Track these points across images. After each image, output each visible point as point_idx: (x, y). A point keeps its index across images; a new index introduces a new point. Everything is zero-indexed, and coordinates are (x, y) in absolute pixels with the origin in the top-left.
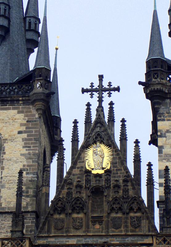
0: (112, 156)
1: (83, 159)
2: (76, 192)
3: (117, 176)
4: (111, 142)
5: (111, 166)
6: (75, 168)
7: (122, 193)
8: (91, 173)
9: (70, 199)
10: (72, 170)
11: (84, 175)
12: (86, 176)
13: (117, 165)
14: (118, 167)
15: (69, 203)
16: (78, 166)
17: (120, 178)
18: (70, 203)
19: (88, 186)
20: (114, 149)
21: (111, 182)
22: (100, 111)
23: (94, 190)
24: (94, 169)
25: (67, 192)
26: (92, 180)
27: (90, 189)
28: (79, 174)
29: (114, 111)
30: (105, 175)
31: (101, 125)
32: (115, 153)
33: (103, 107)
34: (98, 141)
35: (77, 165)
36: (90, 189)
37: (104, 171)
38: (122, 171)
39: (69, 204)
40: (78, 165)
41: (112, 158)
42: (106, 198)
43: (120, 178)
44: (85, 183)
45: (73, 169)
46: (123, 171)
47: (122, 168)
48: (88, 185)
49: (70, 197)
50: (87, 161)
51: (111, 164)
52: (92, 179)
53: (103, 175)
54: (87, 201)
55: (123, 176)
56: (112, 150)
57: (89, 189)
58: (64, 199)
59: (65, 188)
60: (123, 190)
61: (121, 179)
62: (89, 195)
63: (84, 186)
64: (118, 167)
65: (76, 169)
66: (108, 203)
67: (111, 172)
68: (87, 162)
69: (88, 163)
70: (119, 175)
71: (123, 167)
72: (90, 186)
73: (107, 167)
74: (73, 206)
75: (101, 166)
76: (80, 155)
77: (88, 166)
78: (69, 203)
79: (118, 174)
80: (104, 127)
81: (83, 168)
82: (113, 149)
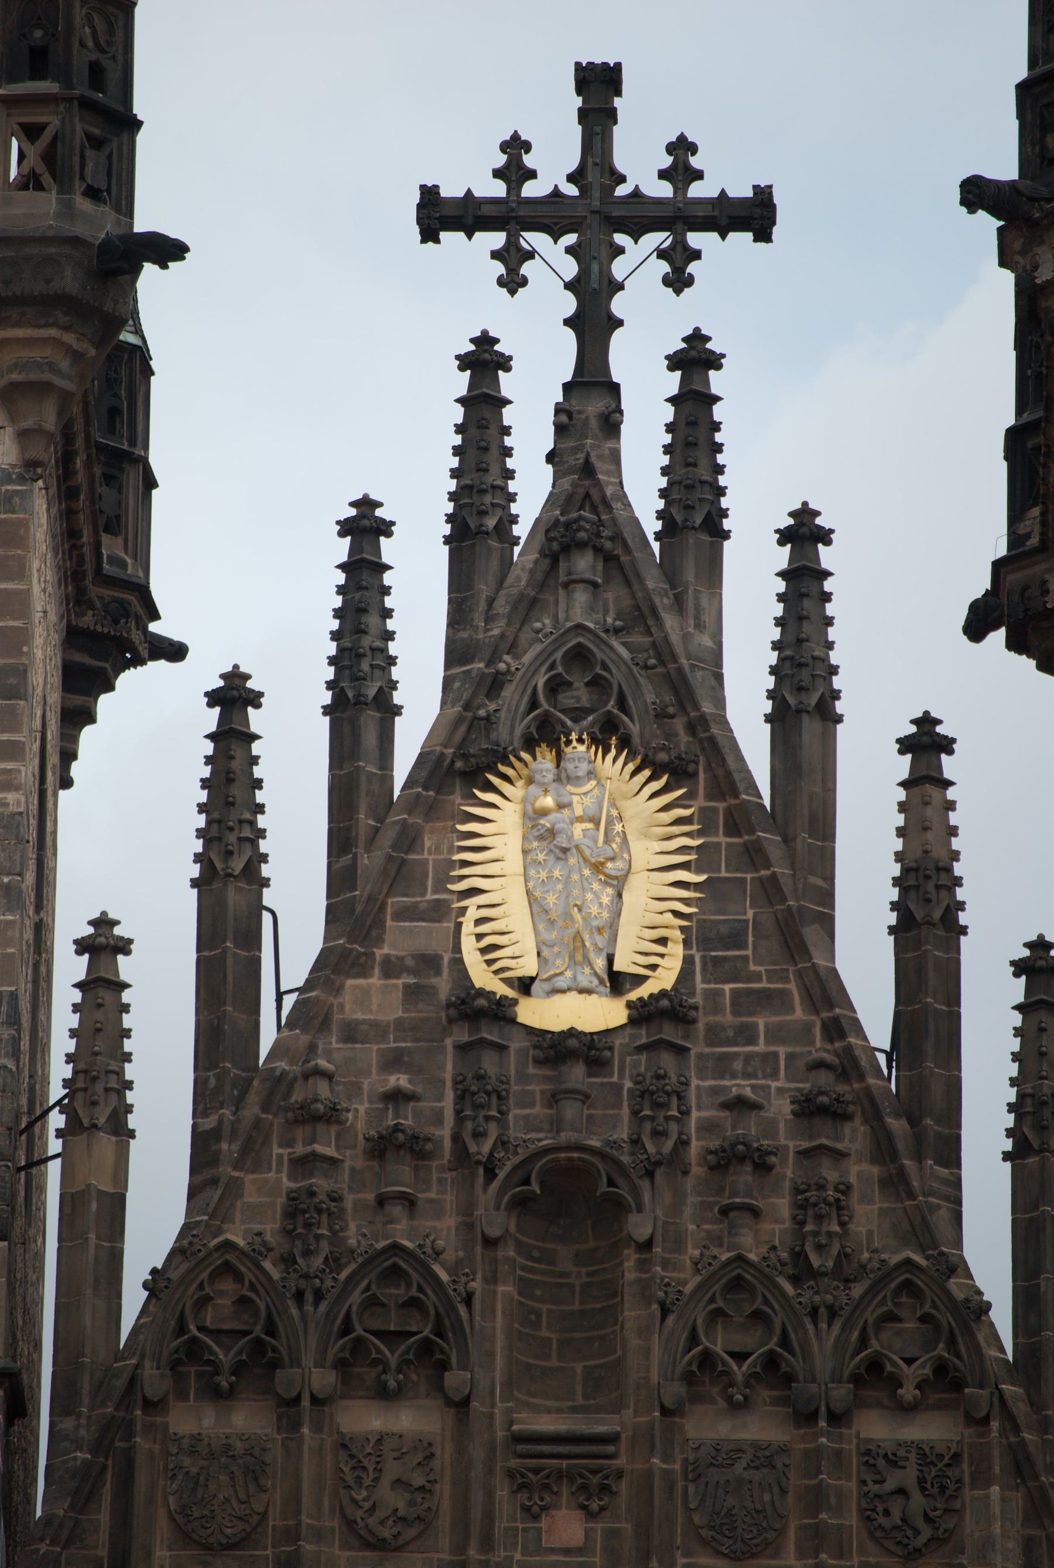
0: (699, 871)
1: (441, 885)
2: (370, 1196)
3: (749, 1058)
4: (691, 728)
5: (688, 961)
6: (364, 972)
7: (788, 1225)
8: (513, 1021)
9: (318, 1262)
10: (338, 991)
11: (449, 1042)
12: (462, 1048)
13: (749, 952)
14: (757, 977)
15: (309, 1297)
16: (386, 950)
17: (774, 1075)
18: (319, 1296)
19: (486, 1147)
20: (721, 806)
21: (686, 1113)
22: (594, 423)
23: (535, 1187)
24: (536, 987)
25: (292, 1197)
26: (515, 1088)
27: (502, 1174)
28: (399, 1023)
29: (716, 427)
30: (640, 1049)
31: (600, 566)
32: (722, 839)
33: (614, 389)
34: (577, 714)
35: (380, 941)
36: (502, 1174)
37: (629, 1005)
38: (791, 1009)
39: (309, 1308)
40: (388, 937)
41: (696, 886)
42: (643, 1265)
43: (774, 1075)
44: (459, 1117)
45: (348, 976)
46: (799, 1013)
47: (792, 986)
48: (479, 1135)
49: (325, 1247)
50: (472, 902)
51: (686, 943)
52: (523, 1077)
53: (618, 1042)
54: (476, 1285)
55: (801, 1064)
56: (702, 810)
57: (490, 1174)
58: (267, 1265)
59: (276, 1150)
60: (797, 1191)
61: (780, 1091)
62: (494, 1232)
63: (447, 1144)
64: (757, 977)
65: (375, 980)
66: (665, 1312)
67: (694, 1021)
68: (472, 914)
69: (479, 922)
70: (761, 1047)
71: (799, 974)
72: (502, 1143)
73: (654, 967)
74: (347, 1328)
75: (600, 963)
76: (409, 850)
77: (484, 951)
78: (309, 1297)
79: (752, 1040)
80: (628, 583)
81: (438, 973)
82: (709, 797)
